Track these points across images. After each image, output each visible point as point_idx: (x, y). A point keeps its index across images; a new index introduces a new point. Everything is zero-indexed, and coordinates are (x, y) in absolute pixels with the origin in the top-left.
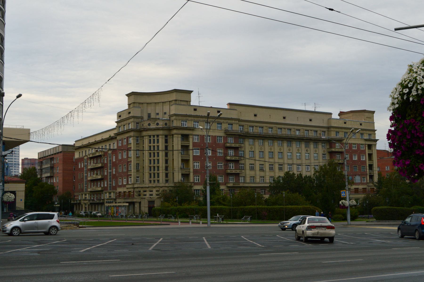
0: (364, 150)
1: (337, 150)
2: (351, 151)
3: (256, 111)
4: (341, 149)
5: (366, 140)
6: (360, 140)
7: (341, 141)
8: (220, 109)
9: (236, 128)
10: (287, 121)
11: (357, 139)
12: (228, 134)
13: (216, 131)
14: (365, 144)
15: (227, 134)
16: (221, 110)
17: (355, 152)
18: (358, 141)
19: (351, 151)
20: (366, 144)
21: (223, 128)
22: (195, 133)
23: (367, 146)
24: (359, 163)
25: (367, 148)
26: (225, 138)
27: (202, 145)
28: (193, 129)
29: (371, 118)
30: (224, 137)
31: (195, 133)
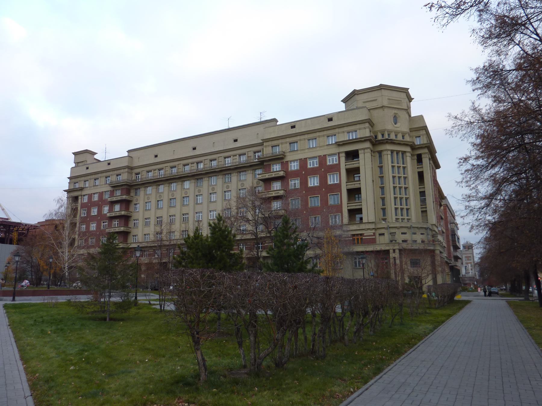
0: (336, 164)
1: (273, 175)
2: (303, 172)
3: (156, 151)
4: (268, 174)
5: (339, 144)
6: (326, 147)
7: (282, 158)
8: (109, 161)
9: (124, 177)
10: (197, 152)
11: (318, 149)
12: (115, 187)
13: (104, 186)
14: (339, 153)
15: (112, 187)
16: (111, 161)
17: (313, 172)
18: (321, 150)
19: (303, 172)
20: (342, 152)
21: (108, 182)
22: (83, 193)
23: (344, 155)
24: (324, 189)
25: (343, 159)
26: (112, 194)
27: (89, 205)
28: (82, 189)
29: (376, 100)
30: (111, 191)
31: (84, 193)
